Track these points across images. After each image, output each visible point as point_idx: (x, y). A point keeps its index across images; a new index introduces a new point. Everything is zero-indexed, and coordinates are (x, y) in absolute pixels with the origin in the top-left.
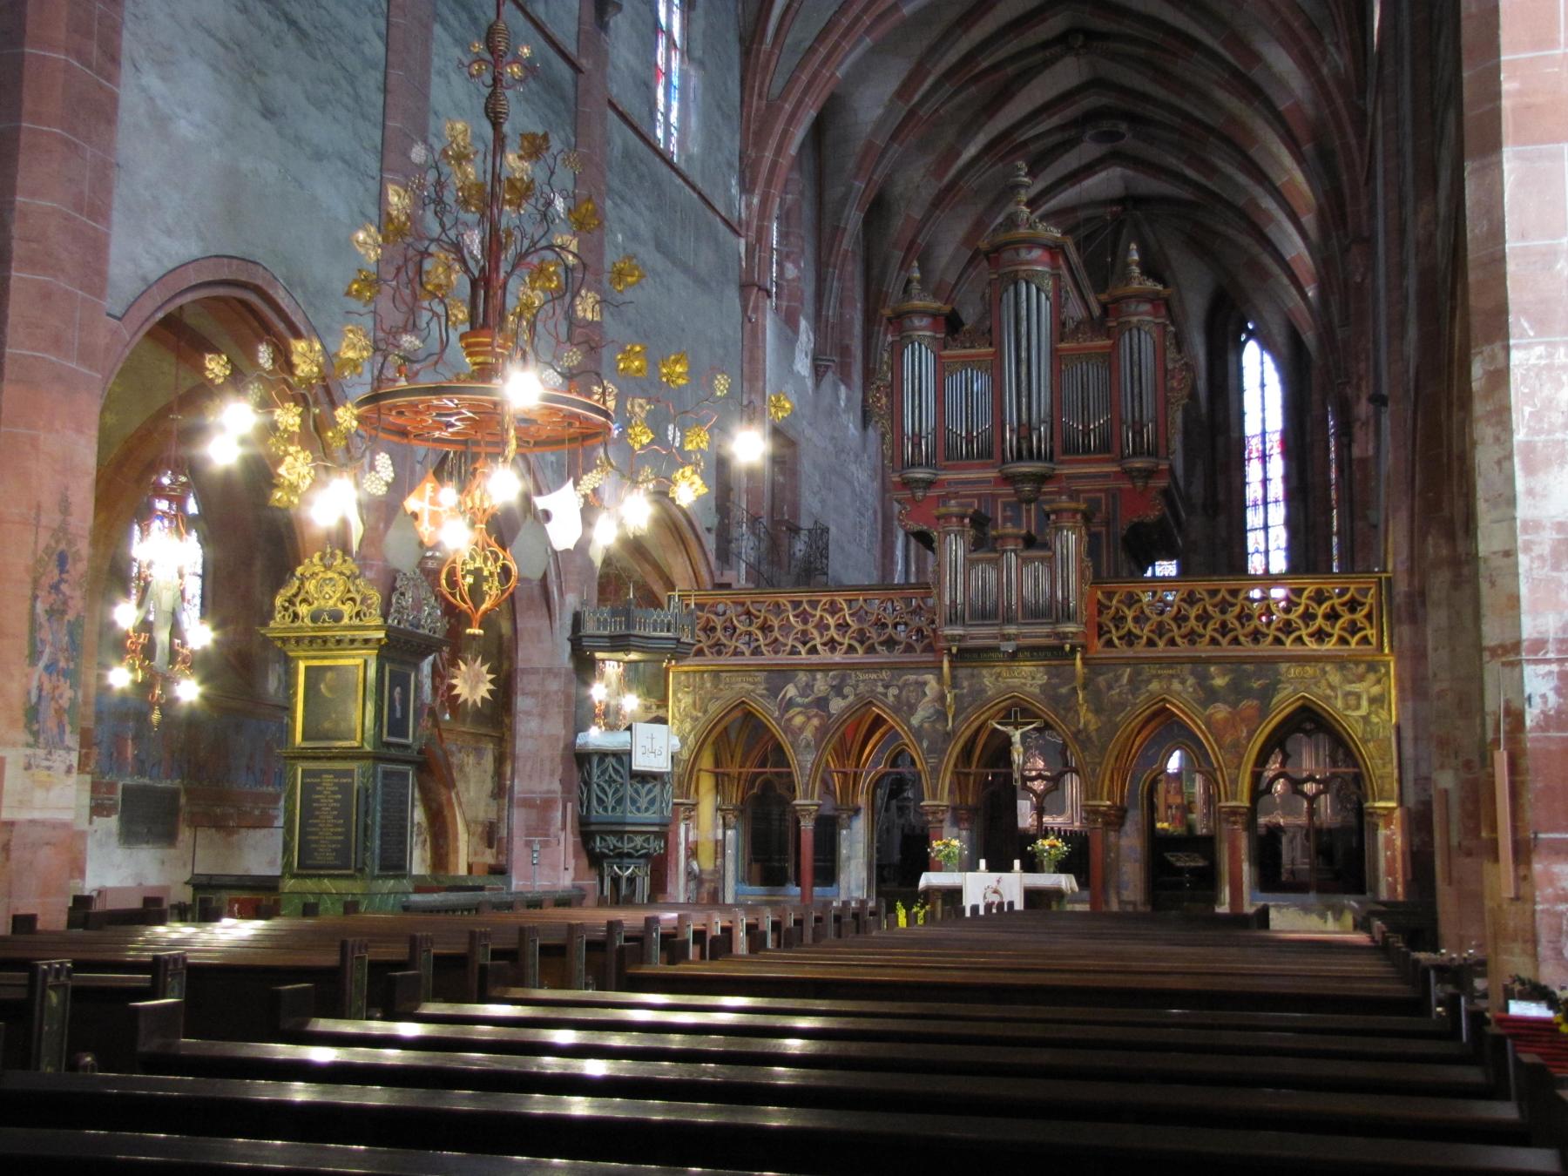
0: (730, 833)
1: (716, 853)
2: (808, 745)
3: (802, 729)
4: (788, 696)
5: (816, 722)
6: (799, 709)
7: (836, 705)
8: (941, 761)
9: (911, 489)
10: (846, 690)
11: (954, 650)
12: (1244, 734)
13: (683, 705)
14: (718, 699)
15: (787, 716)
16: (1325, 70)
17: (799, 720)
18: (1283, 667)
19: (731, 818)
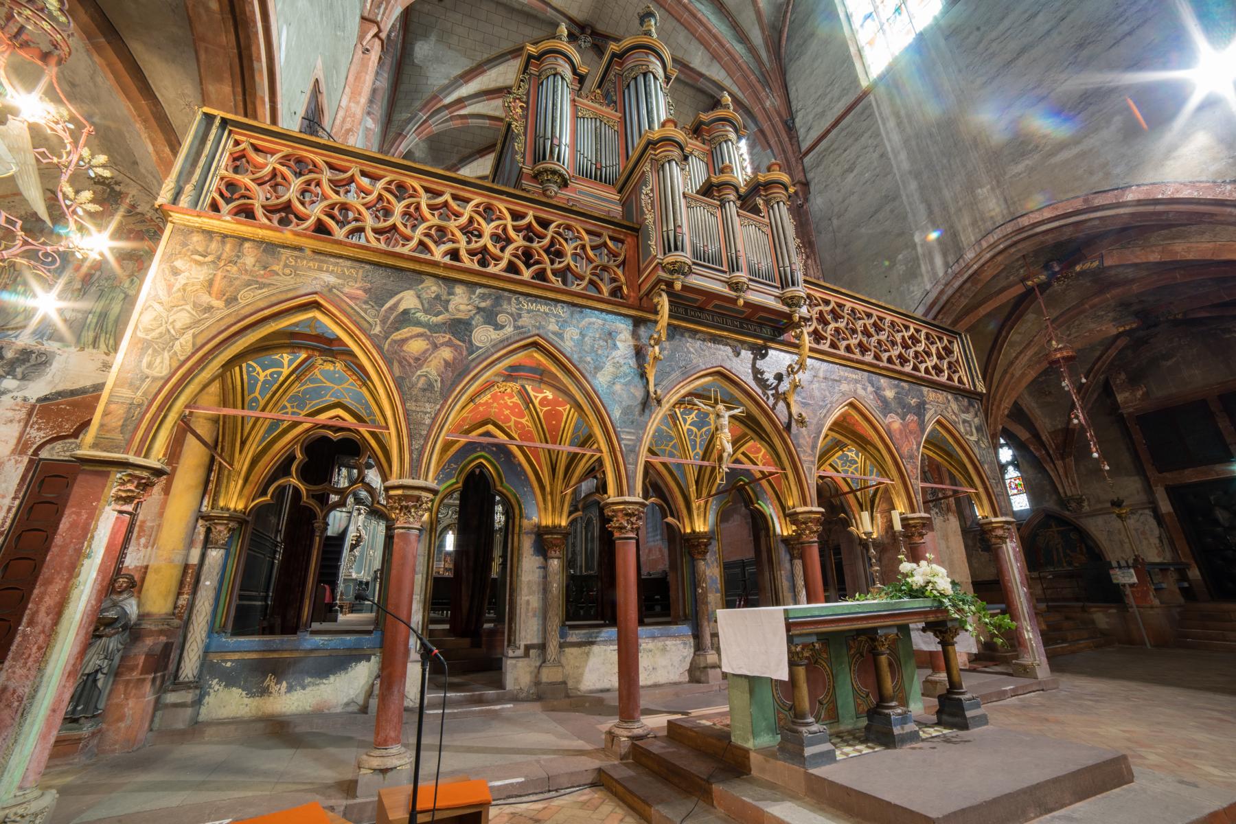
0: (215, 555)
1: (181, 584)
2: (430, 386)
3: (420, 360)
4: (401, 308)
5: (446, 353)
6: (420, 330)
7: (483, 335)
8: (640, 440)
9: (542, 183)
10: (501, 318)
11: (678, 286)
12: (915, 447)
13: (182, 280)
14: (262, 286)
15: (397, 336)
16: (768, 104)
17: (416, 347)
18: (925, 390)
19: (222, 533)
